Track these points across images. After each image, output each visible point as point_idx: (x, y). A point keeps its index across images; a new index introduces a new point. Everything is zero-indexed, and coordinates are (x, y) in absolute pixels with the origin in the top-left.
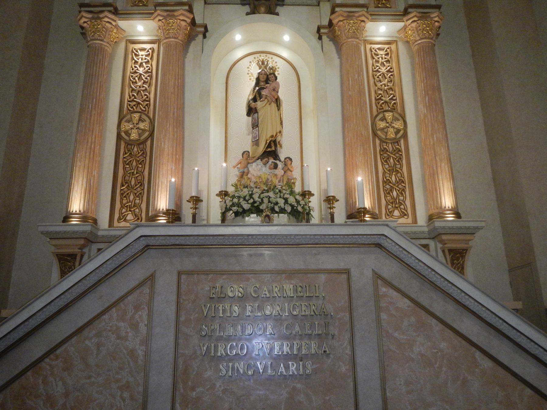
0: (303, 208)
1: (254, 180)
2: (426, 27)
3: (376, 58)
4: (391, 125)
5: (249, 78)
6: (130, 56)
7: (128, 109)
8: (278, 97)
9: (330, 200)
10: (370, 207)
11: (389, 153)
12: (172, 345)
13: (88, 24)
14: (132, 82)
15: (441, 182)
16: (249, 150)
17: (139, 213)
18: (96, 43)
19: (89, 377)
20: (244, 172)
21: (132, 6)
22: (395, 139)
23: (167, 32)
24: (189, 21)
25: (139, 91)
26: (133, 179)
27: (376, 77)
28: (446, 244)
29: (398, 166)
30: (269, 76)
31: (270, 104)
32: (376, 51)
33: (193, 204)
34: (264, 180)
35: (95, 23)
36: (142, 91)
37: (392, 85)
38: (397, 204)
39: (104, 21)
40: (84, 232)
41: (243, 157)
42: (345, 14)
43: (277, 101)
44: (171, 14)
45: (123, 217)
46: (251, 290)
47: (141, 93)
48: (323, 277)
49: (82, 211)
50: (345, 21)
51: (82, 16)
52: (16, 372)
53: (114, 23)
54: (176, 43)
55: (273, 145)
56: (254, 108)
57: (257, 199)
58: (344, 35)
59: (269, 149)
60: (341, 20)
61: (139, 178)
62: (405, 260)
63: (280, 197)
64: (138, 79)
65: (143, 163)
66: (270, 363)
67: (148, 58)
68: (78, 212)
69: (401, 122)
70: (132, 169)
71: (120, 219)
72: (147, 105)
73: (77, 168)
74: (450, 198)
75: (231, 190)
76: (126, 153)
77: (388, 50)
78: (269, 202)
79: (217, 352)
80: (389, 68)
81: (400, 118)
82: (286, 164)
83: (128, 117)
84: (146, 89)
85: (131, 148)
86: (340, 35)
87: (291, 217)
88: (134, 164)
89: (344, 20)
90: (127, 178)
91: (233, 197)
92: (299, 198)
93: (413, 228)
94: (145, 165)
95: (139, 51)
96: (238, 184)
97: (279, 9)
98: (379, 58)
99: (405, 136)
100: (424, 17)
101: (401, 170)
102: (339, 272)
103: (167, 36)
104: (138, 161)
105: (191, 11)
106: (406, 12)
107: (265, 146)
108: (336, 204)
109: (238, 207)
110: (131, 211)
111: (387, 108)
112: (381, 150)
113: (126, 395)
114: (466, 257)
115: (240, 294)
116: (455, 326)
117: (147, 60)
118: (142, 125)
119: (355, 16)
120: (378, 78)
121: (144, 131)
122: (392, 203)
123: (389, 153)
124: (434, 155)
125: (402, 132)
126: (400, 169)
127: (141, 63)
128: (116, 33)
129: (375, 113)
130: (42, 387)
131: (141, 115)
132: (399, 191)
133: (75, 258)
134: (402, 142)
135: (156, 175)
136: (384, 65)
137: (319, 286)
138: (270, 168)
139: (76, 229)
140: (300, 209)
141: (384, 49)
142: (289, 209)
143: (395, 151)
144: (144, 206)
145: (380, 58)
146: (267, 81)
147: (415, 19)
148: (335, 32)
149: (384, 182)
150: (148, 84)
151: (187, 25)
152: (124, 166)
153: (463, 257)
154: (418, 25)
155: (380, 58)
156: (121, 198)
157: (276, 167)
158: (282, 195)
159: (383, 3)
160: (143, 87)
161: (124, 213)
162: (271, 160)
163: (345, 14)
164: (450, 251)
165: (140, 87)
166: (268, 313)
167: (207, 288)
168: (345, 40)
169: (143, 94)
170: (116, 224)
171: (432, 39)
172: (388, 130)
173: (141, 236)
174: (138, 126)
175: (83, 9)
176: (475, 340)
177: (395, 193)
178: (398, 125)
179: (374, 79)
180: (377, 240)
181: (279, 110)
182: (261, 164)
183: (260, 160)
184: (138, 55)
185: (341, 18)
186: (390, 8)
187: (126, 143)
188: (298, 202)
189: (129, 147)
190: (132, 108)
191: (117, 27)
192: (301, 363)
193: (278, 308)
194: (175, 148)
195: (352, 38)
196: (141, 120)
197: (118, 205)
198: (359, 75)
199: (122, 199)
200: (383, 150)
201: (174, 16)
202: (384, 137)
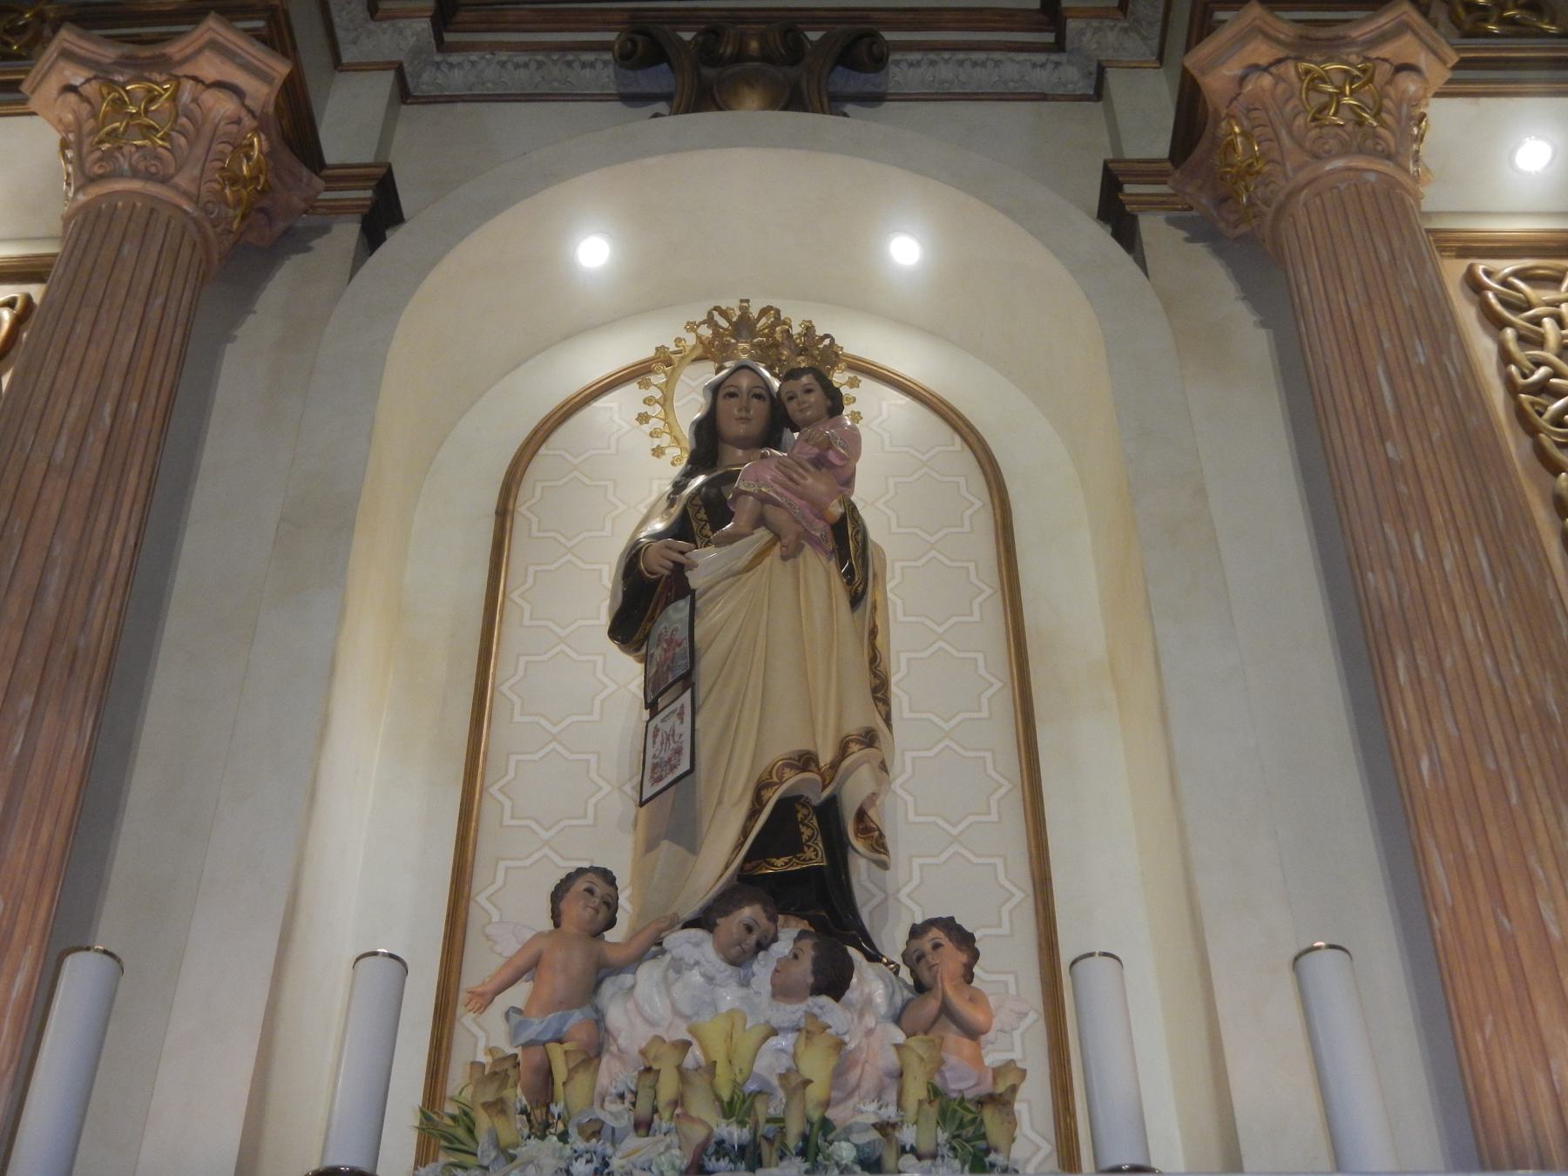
8: (852, 508)
23: (105, 147)
24: (260, 93)
41: (556, 916)
50: (1289, 70)
54: (153, 207)
55: (809, 830)
58: (1287, 142)
59: (780, 864)
60: (1263, 61)
82: (926, 976)
89: (1279, 61)
98: (1537, 321)
107: (745, 833)
119: (1353, 43)
145: (1548, 323)
151: (248, 122)
168: (1299, 168)
201: (163, 63)
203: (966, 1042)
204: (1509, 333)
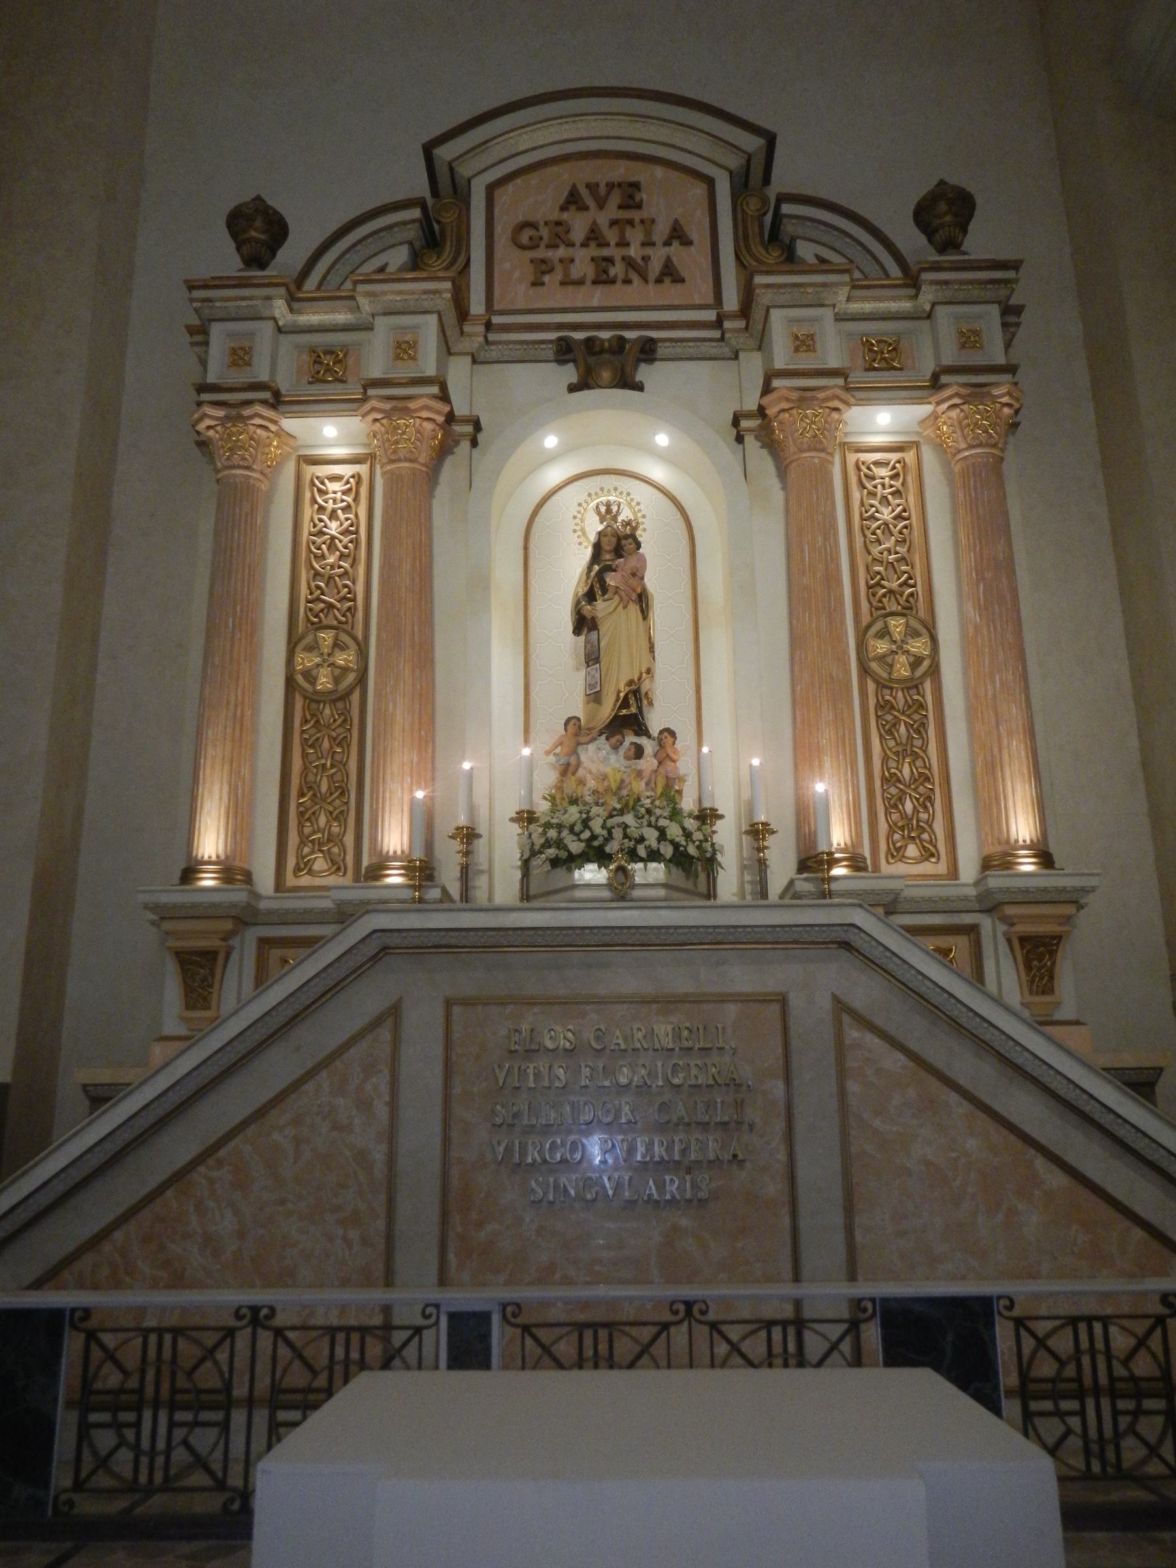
0: (698, 847)
1: (591, 784)
2: (982, 419)
3: (869, 485)
4: (902, 648)
5: (577, 540)
6: (308, 495)
7: (308, 620)
8: (644, 589)
9: (757, 832)
10: (849, 843)
11: (896, 713)
12: (438, 1140)
13: (217, 432)
14: (315, 557)
15: (1009, 784)
16: (580, 715)
17: (340, 855)
18: (235, 476)
19: (283, 1202)
20: (568, 765)
21: (310, 383)
22: (912, 679)
24: (440, 419)
25: (331, 578)
26: (325, 779)
27: (868, 533)
28: (1012, 925)
29: (918, 743)
30: (623, 542)
31: (625, 607)
32: (869, 468)
33: (462, 842)
34: (614, 786)
35: (234, 429)
36: (337, 578)
37: (905, 550)
39: (254, 425)
40: (233, 905)
41: (566, 730)
42: (795, 395)
43: (642, 600)
44: (400, 407)
45: (304, 866)
46: (589, 1035)
47: (335, 581)
48: (731, 1009)
49: (222, 857)
50: (794, 412)
51: (205, 415)
52: (144, 1191)
53: (273, 428)
55: (632, 701)
56: (589, 616)
57: (598, 830)
58: (792, 444)
59: (624, 712)
60: (786, 407)
61: (338, 777)
62: (898, 974)
63: (649, 825)
64: (328, 549)
65: (343, 742)
66: (627, 1178)
67: (349, 499)
68: (214, 858)
69: (925, 639)
70: (322, 758)
71: (300, 870)
72: (349, 609)
73: (209, 762)
74: (1028, 820)
75: (542, 807)
76: (307, 722)
77: (897, 465)
78: (626, 836)
79: (526, 1155)
81: (924, 631)
83: (310, 638)
84: (346, 573)
85: (318, 709)
86: (783, 441)
87: (674, 869)
88: (326, 744)
89: (791, 409)
90: (311, 778)
91: (548, 826)
92: (691, 824)
93: (945, 889)
94: (349, 746)
95: (326, 481)
96: (558, 797)
97: (644, 373)
98: (875, 487)
99: (935, 671)
100: (977, 394)
101: (925, 752)
102: (764, 999)
103: (393, 457)
104: (335, 739)
105: (444, 397)
106: (935, 384)
107: (615, 706)
108: (770, 841)
109: (558, 848)
110: (322, 852)
111: (894, 607)
112: (879, 706)
113: (353, 1234)
114: (1059, 954)
115: (568, 1044)
116: (997, 1107)
117: (345, 504)
118: (341, 659)
119: (817, 399)
120: (874, 533)
121: (345, 670)
122: (902, 828)
123: (896, 713)
124: (994, 722)
126: (921, 748)
127: (334, 511)
128: (277, 447)
129: (866, 619)
130: (194, 1218)
131: (337, 634)
132: (917, 800)
133: (215, 959)
134: (928, 685)
135: (378, 777)
137: (723, 1028)
138: (627, 758)
139: (217, 898)
140: (692, 850)
141: (888, 464)
142: (667, 851)
143: (910, 707)
144: (349, 840)
145: (879, 486)
146: (618, 551)
147: (956, 401)
148: (773, 432)
149: (884, 780)
150: (350, 560)
151: (437, 428)
152: (303, 750)
153: (1052, 953)
154: (962, 414)
155: (879, 486)
156: (299, 823)
157: (639, 752)
158: (653, 819)
159: (885, 359)
160: (340, 567)
161: (306, 856)
162: (630, 738)
163: (795, 395)
164: (1023, 940)
165: (332, 567)
166: (623, 1080)
167: (503, 1032)
168: (795, 453)
169: (339, 584)
170: (291, 881)
171: (994, 446)
172: (893, 659)
173: (375, 931)
174: (331, 660)
175: (205, 397)
176: (1036, 1134)
177: (909, 806)
178: (919, 646)
179: (865, 536)
180: (841, 935)
182: (608, 747)
183: (604, 737)
184: (326, 493)
185: (785, 405)
186: (901, 369)
187: (305, 698)
188: (688, 835)
189: (314, 706)
190: (316, 616)
191: (281, 434)
192: (688, 1178)
193: (643, 1072)
194: (416, 716)
195: (810, 449)
196: (338, 645)
197: (293, 839)
198: (825, 539)
199: (301, 826)
200: (884, 706)
201: (406, 412)
202: (885, 675)
203: (673, 764)
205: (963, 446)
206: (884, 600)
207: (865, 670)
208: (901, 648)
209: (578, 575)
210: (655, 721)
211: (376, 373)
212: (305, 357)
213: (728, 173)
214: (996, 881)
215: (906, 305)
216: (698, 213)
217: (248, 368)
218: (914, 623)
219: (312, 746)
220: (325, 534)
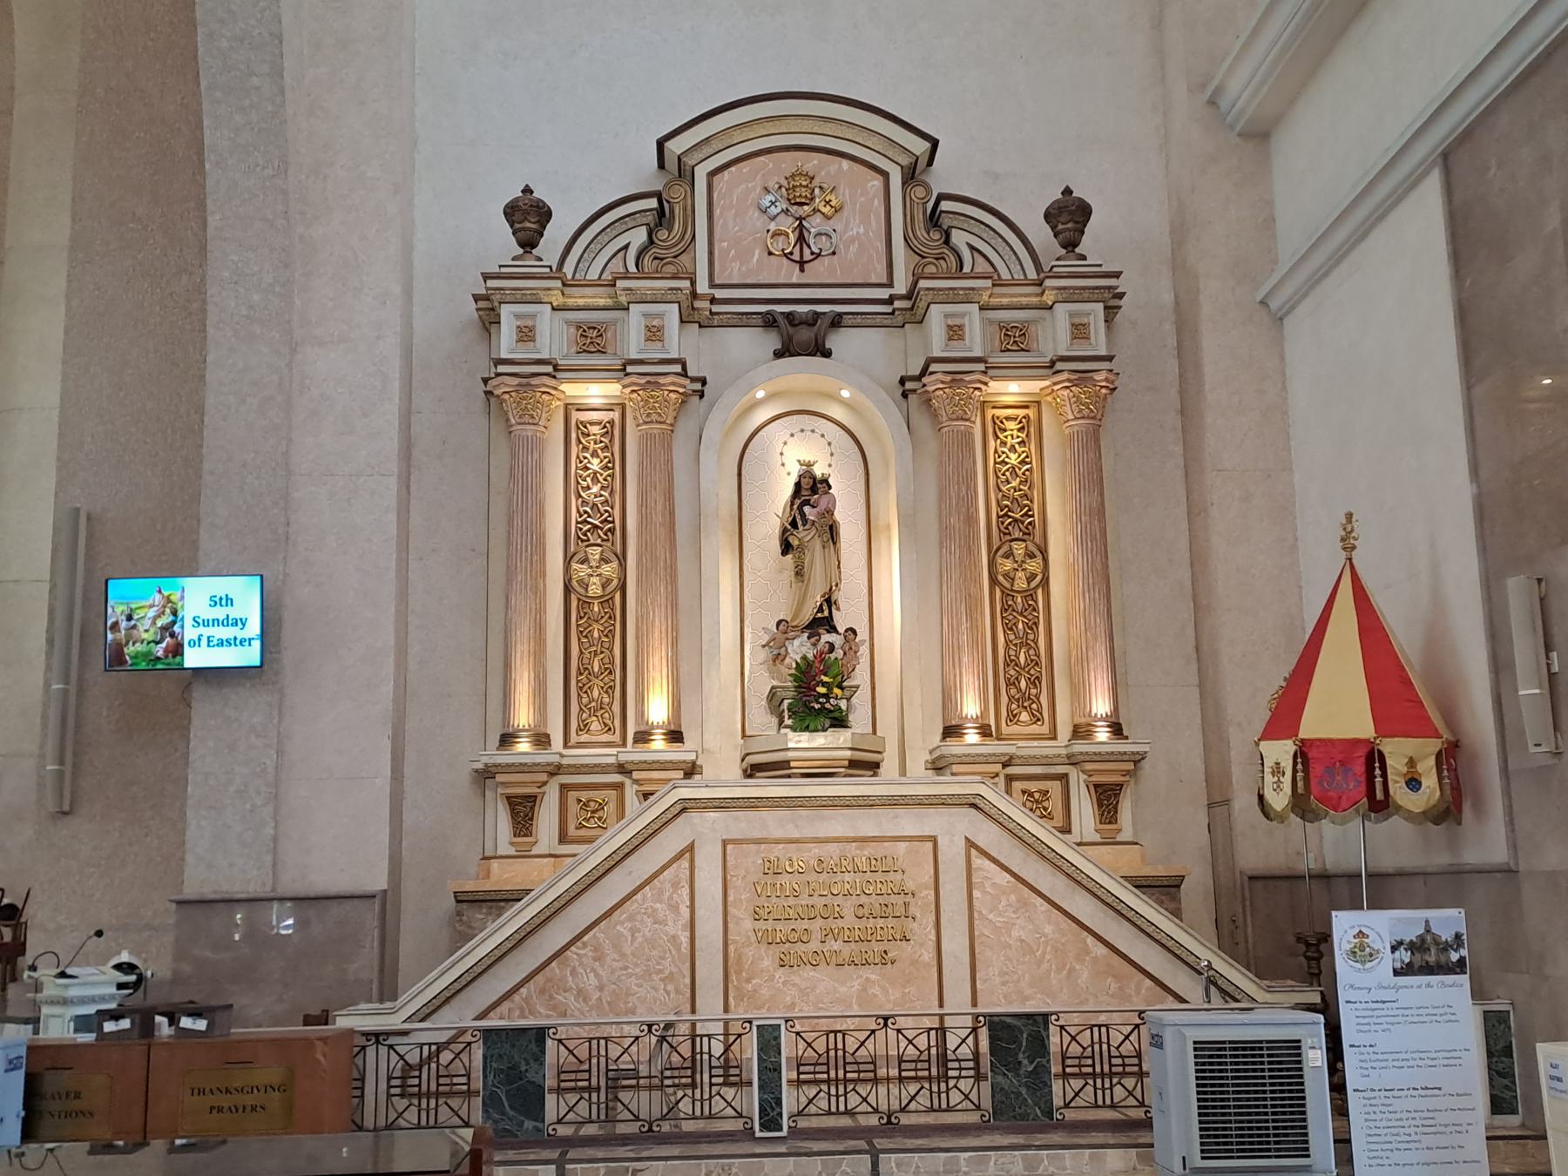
6: (574, 435)
7: (579, 538)
27: (1000, 474)
32: (1002, 422)
37: (1026, 488)
38: (1025, 701)
43: (832, 531)
69: (1039, 559)
72: (609, 530)
80: (1024, 455)
81: (1038, 553)
94: (613, 637)
97: (835, 341)
99: (1045, 582)
100: (1082, 378)
101: (1036, 644)
103: (647, 420)
111: (1017, 534)
112: (1004, 610)
120: (1004, 475)
125: (1039, 578)
129: (996, 543)
134: (1040, 591)
136: (1016, 451)
141: (1016, 419)
144: (616, 708)
146: (814, 490)
149: (1007, 665)
152: (579, 639)
156: (579, 695)
159: (1015, 342)
160: (601, 496)
169: (602, 509)
170: (574, 738)
171: (1094, 418)
175: (501, 369)
178: (1034, 566)
179: (998, 477)
181: (834, 543)
182: (809, 644)
185: (941, 386)
202: (1008, 586)
204: (999, 441)
205: (1071, 417)
206: (1010, 528)
207: (993, 581)
208: (1020, 566)
209: (784, 502)
210: (841, 623)
211: (634, 356)
212: (573, 330)
213: (899, 168)
214: (1080, 747)
215: (1035, 300)
216: (876, 201)
217: (532, 343)
218: (1032, 548)
219: (586, 637)
220: (588, 469)
